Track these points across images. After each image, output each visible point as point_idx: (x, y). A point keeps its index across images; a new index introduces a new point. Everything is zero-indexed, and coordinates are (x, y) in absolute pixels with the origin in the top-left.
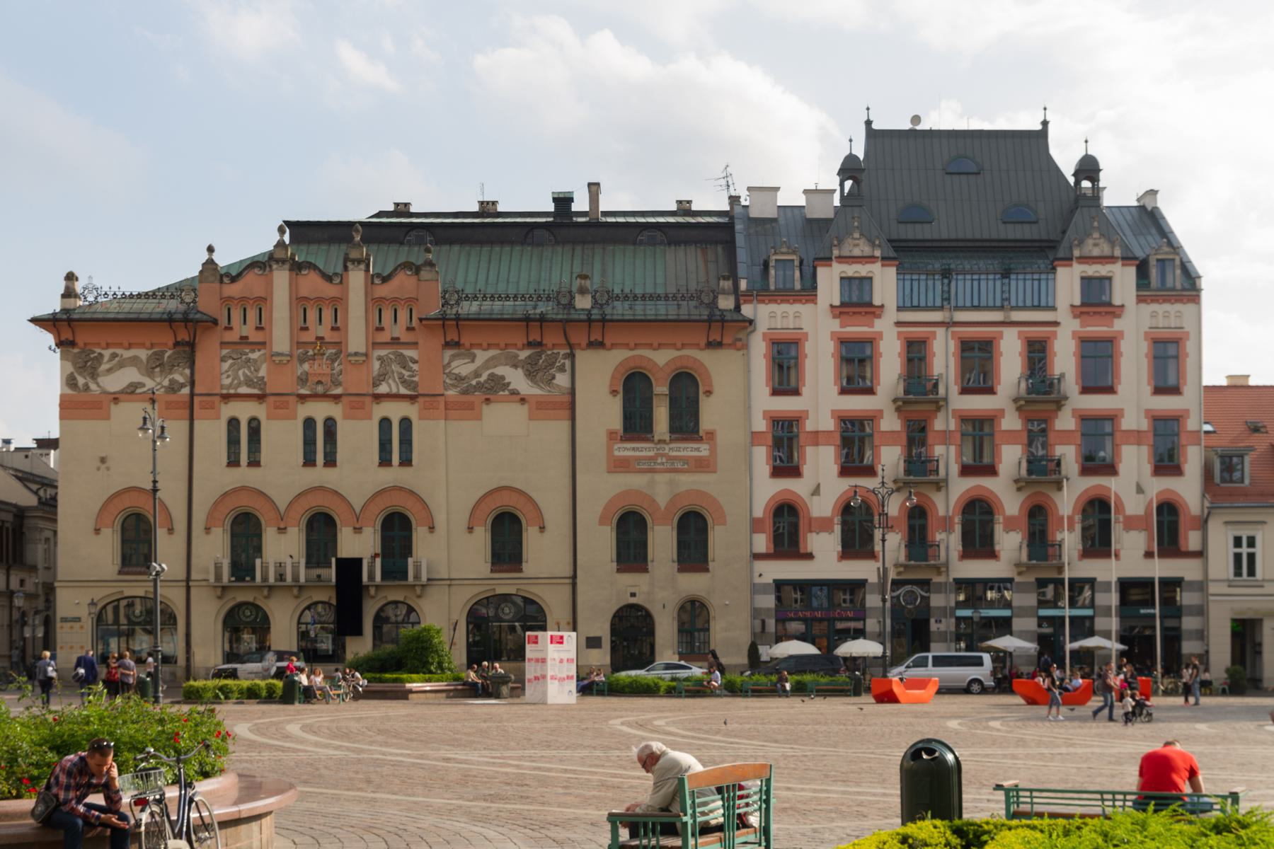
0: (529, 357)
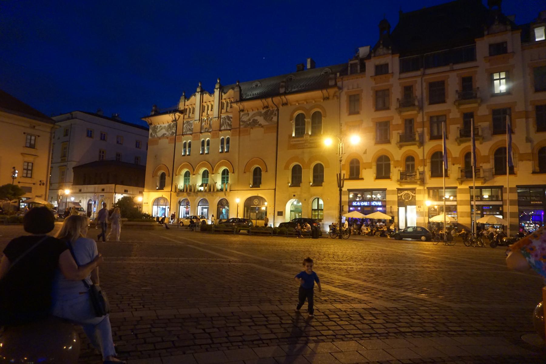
0: (265, 112)
